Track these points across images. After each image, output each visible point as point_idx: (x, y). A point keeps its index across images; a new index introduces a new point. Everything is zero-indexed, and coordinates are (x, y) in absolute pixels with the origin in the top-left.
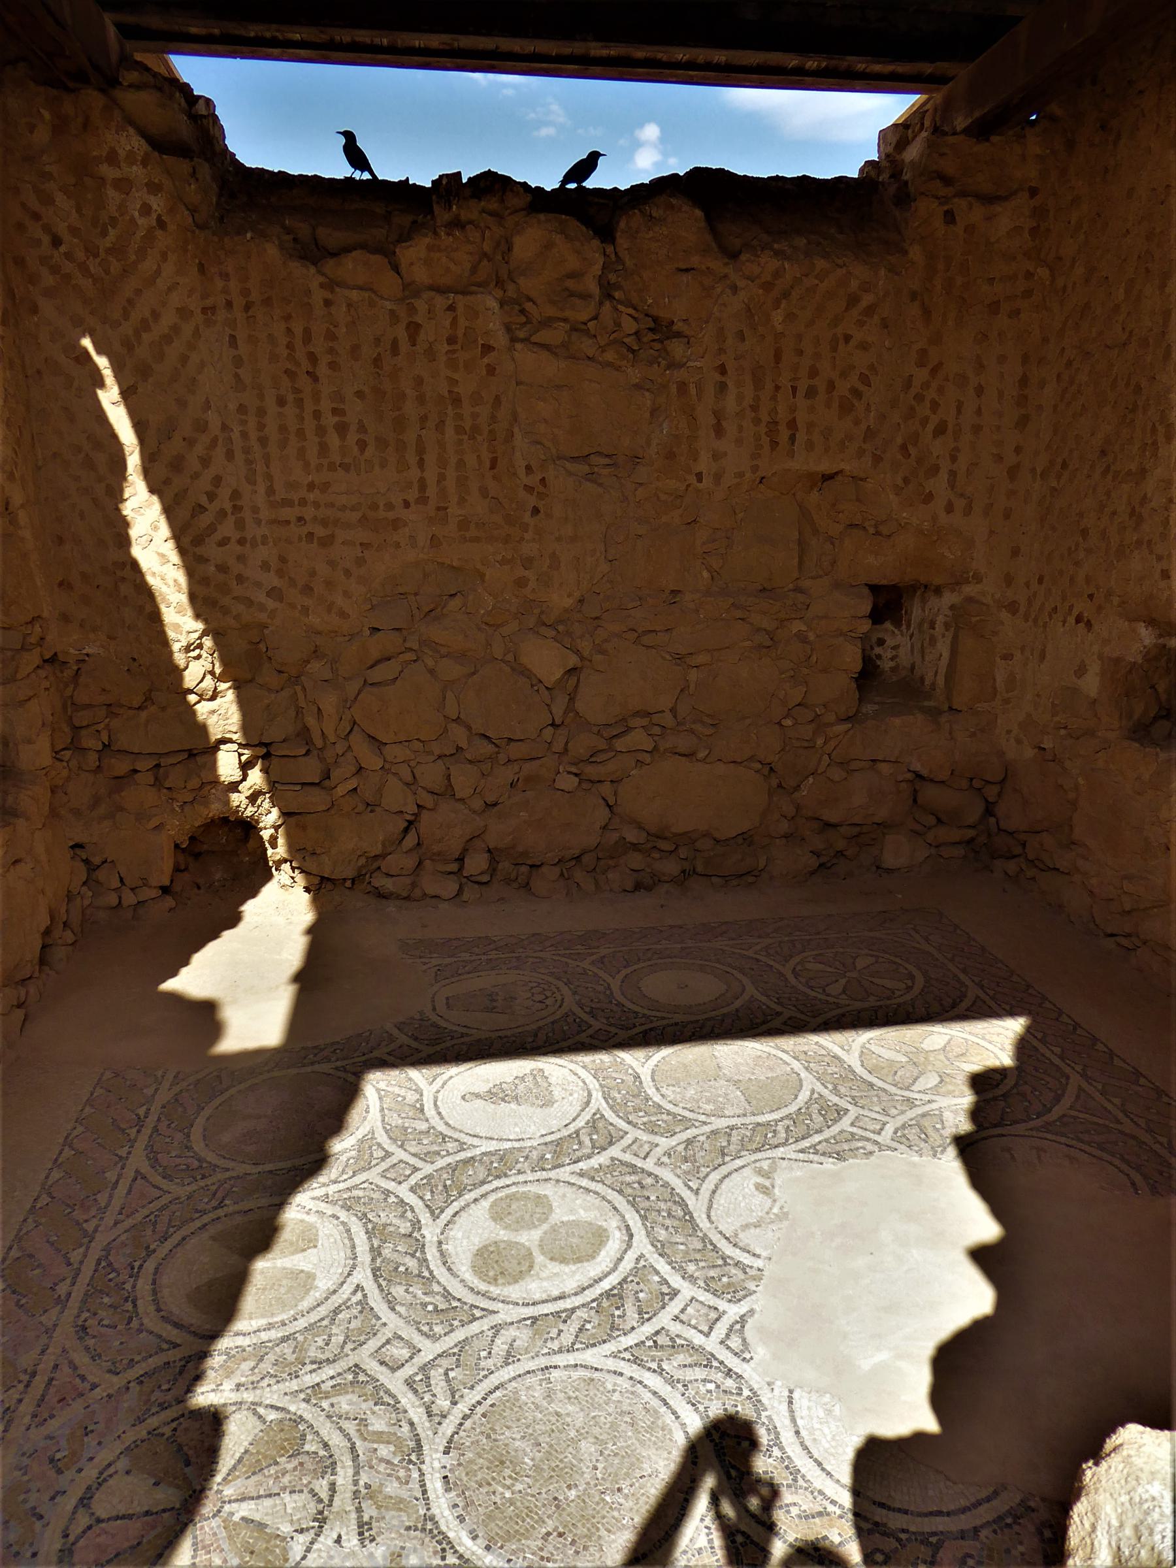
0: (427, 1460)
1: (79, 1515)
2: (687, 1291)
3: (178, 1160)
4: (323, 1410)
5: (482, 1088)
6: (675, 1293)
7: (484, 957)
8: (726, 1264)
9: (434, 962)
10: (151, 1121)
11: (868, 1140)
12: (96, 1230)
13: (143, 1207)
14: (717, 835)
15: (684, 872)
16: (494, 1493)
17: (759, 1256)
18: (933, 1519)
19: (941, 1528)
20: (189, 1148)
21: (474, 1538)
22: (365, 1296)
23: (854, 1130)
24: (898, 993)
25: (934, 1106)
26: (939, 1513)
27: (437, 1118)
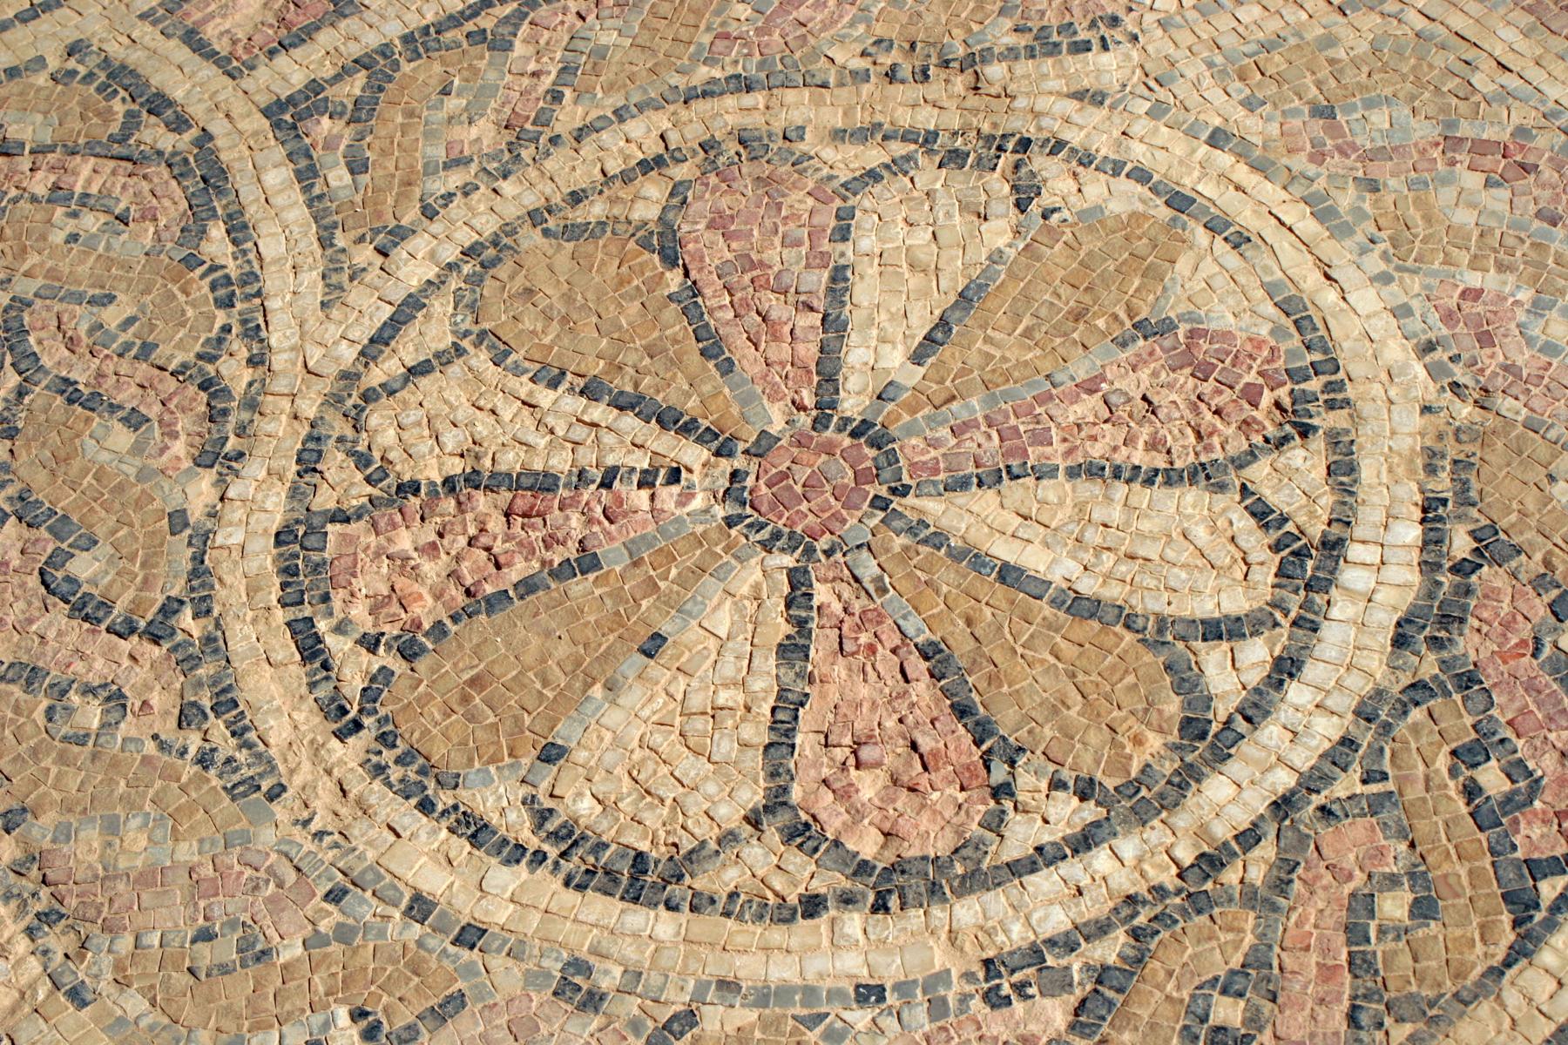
4: (467, 190)
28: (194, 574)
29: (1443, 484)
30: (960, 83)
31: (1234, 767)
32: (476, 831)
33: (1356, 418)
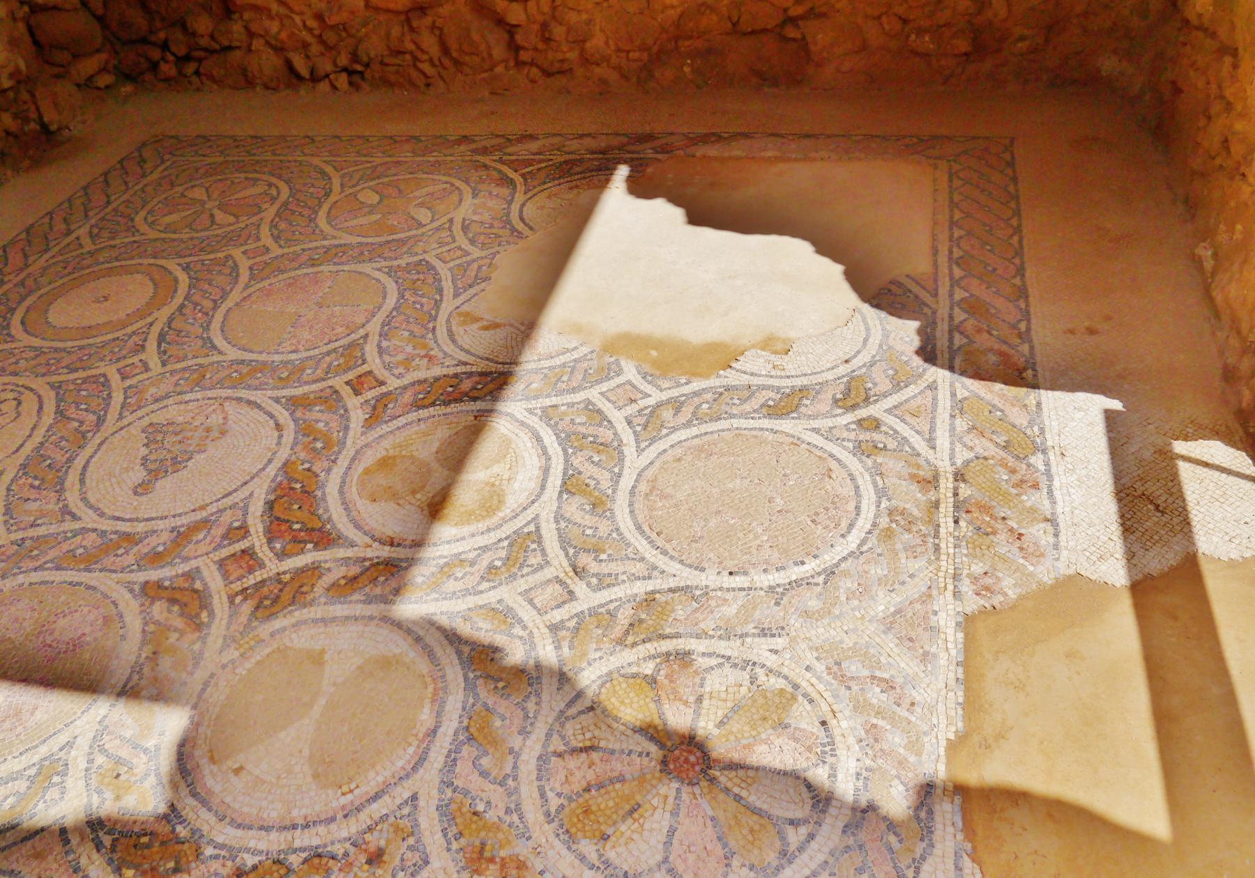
4: (601, 658)
21: (803, 563)
28: (514, 768)
29: (860, 783)
30: (739, 642)
31: (794, 866)
32: (582, 858)
33: (838, 761)
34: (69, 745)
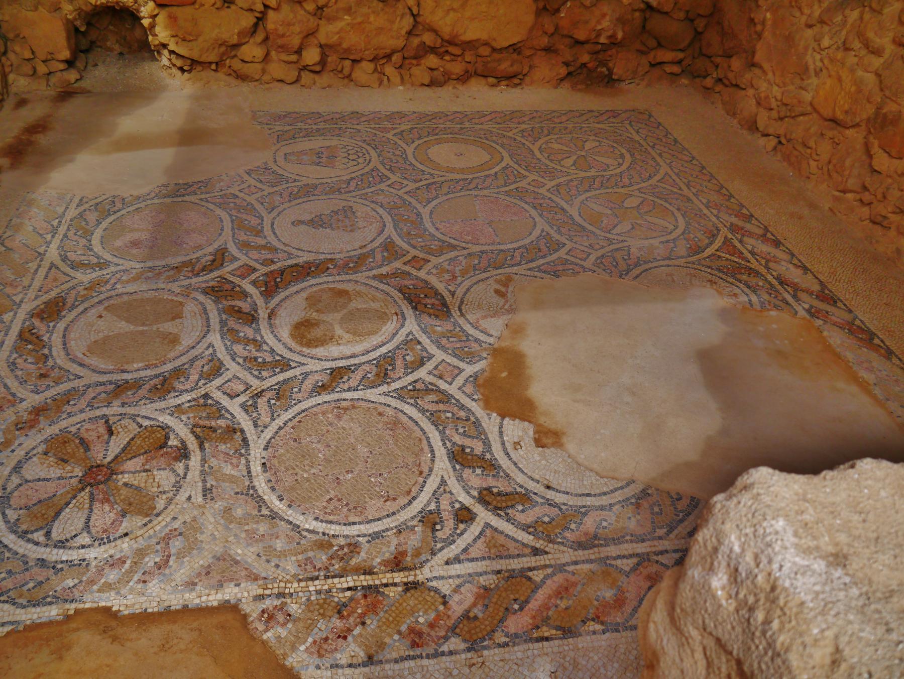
0: (252, 452)
1: (13, 478)
2: (439, 355)
3: (83, 258)
5: (307, 217)
6: (430, 357)
7: (315, 127)
8: (468, 340)
9: (278, 128)
10: (62, 229)
11: (576, 264)
12: (21, 302)
13: (57, 287)
14: (494, 44)
15: (467, 72)
16: (296, 474)
17: (491, 336)
18: (584, 498)
19: (589, 503)
20: (91, 250)
21: (281, 500)
22: (215, 351)
23: (569, 257)
24: (612, 168)
25: (626, 244)
26: (588, 495)
27: (273, 236)
34: (118, 265)
